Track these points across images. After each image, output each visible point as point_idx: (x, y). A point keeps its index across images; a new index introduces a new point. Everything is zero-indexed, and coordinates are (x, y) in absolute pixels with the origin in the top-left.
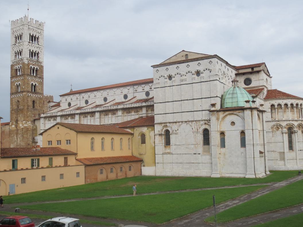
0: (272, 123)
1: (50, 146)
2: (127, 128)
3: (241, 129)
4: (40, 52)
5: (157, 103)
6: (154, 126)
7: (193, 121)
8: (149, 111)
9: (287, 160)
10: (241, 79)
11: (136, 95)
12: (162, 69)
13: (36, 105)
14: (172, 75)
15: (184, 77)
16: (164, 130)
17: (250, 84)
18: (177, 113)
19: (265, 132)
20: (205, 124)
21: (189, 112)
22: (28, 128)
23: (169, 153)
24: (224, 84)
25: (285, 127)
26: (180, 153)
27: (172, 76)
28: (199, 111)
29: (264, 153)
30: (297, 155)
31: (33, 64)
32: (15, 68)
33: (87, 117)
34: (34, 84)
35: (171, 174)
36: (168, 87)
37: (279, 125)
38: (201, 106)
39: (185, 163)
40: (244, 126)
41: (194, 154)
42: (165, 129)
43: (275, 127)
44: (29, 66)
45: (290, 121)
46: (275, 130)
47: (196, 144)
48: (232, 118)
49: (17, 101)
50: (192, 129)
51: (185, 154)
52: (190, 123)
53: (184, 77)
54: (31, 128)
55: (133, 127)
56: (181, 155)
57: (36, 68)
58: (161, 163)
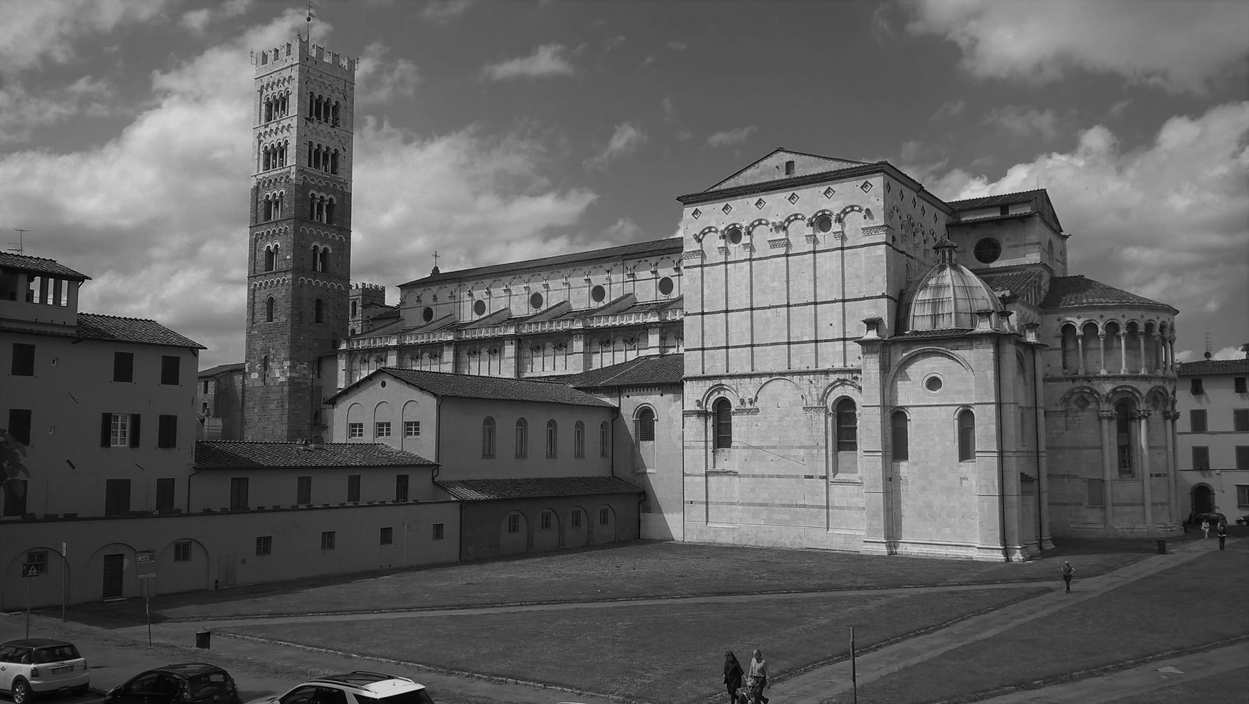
0: (1067, 383)
1: (356, 440)
2: (597, 390)
4: (341, 151)
8: (668, 338)
10: (970, 242)
13: (325, 312)
14: (741, 227)
17: (995, 257)
19: (1041, 412)
20: (843, 382)
22: (298, 383)
24: (907, 255)
25: (1108, 400)
29: (1035, 483)
30: (1147, 490)
33: (480, 353)
34: (321, 248)
35: (734, 539)
37: (1088, 391)
38: (831, 325)
41: (806, 477)
42: (716, 396)
43: (1075, 397)
46: (1074, 407)
47: (812, 447)
51: (779, 476)
52: (796, 378)
54: (311, 385)
55: (617, 390)
56: (766, 480)
58: (701, 503)
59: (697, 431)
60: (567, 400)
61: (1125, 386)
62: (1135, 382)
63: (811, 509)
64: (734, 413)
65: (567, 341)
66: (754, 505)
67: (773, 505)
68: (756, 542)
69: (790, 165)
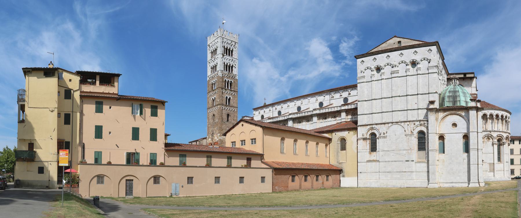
5: (362, 101)
6: (356, 129)
7: (406, 122)
9: (496, 171)
11: (332, 102)
14: (381, 66)
16: (369, 133)
18: (386, 112)
21: (401, 111)
26: (388, 161)
28: (414, 110)
35: (378, 185)
39: (395, 172)
41: (406, 161)
42: (370, 132)
47: (409, 150)
48: (455, 118)
50: (405, 131)
51: (395, 161)
52: (402, 124)
56: (390, 163)
60: (313, 134)
63: (408, 173)
64: (378, 138)
65: (311, 119)
66: (385, 172)
67: (393, 172)
68: (387, 186)
69: (399, 42)
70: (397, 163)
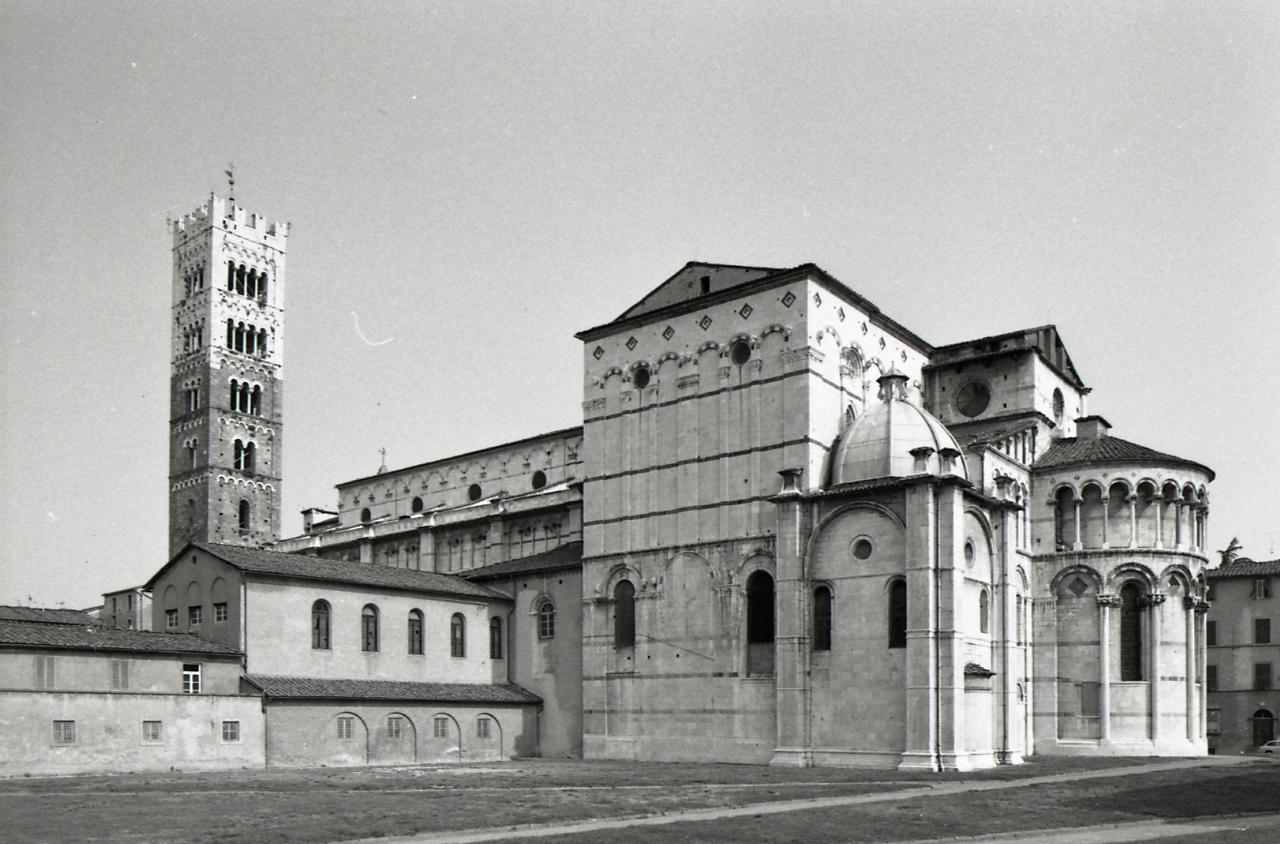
3: (893, 569)
4: (269, 332)
12: (615, 345)
15: (691, 370)
16: (614, 583)
23: (631, 675)
27: (649, 369)
31: (242, 373)
32: (183, 386)
33: (398, 552)
36: (634, 412)
40: (901, 559)
42: (618, 578)
44: (224, 379)
45: (1131, 553)
46: (1069, 592)
49: (187, 503)
50: (712, 574)
53: (691, 370)
57: (252, 385)
59: (599, 623)
61: (1132, 564)
62: (1146, 559)
65: (486, 532)
70: (689, 680)
